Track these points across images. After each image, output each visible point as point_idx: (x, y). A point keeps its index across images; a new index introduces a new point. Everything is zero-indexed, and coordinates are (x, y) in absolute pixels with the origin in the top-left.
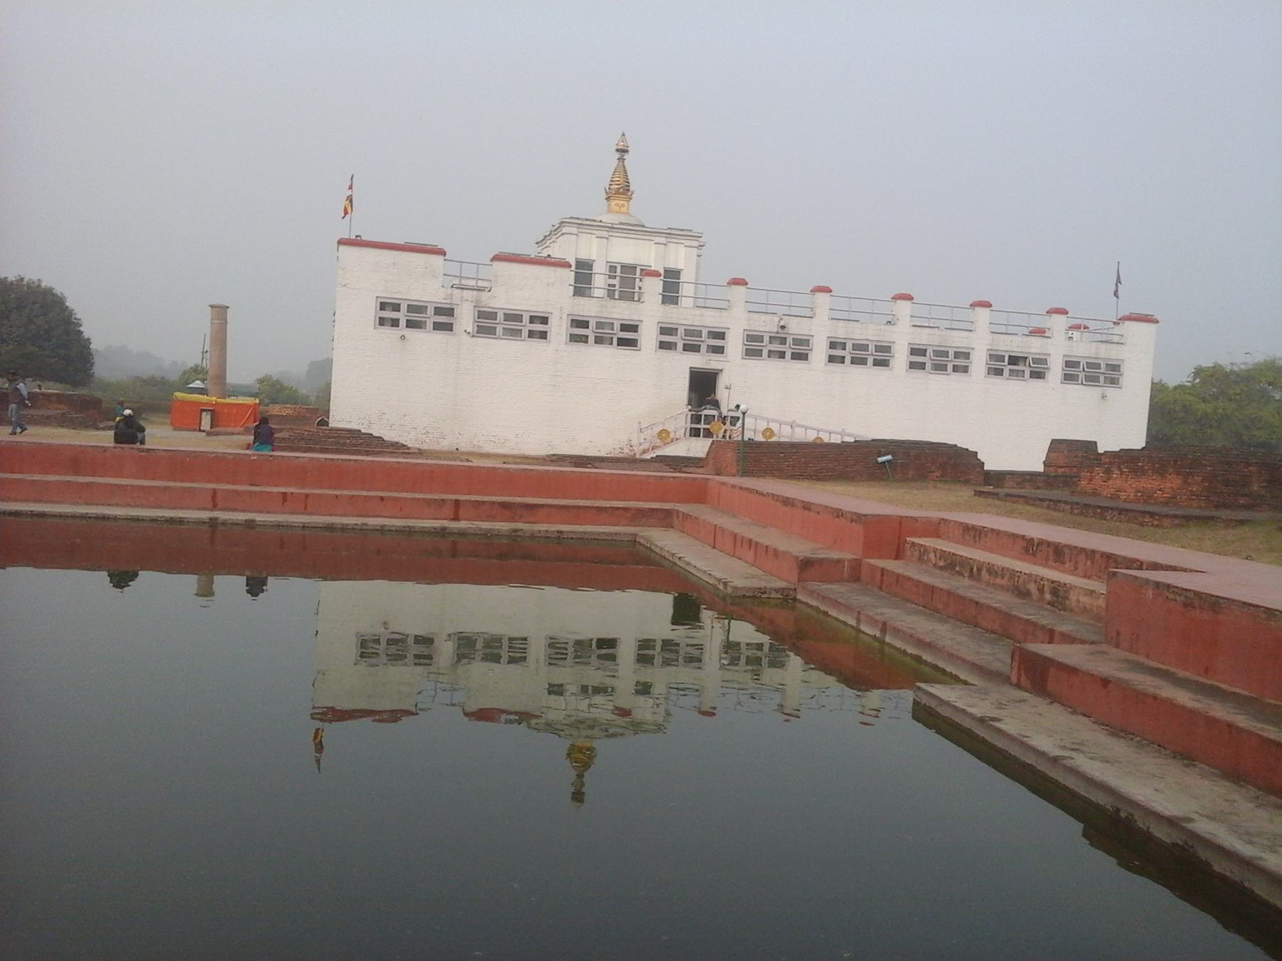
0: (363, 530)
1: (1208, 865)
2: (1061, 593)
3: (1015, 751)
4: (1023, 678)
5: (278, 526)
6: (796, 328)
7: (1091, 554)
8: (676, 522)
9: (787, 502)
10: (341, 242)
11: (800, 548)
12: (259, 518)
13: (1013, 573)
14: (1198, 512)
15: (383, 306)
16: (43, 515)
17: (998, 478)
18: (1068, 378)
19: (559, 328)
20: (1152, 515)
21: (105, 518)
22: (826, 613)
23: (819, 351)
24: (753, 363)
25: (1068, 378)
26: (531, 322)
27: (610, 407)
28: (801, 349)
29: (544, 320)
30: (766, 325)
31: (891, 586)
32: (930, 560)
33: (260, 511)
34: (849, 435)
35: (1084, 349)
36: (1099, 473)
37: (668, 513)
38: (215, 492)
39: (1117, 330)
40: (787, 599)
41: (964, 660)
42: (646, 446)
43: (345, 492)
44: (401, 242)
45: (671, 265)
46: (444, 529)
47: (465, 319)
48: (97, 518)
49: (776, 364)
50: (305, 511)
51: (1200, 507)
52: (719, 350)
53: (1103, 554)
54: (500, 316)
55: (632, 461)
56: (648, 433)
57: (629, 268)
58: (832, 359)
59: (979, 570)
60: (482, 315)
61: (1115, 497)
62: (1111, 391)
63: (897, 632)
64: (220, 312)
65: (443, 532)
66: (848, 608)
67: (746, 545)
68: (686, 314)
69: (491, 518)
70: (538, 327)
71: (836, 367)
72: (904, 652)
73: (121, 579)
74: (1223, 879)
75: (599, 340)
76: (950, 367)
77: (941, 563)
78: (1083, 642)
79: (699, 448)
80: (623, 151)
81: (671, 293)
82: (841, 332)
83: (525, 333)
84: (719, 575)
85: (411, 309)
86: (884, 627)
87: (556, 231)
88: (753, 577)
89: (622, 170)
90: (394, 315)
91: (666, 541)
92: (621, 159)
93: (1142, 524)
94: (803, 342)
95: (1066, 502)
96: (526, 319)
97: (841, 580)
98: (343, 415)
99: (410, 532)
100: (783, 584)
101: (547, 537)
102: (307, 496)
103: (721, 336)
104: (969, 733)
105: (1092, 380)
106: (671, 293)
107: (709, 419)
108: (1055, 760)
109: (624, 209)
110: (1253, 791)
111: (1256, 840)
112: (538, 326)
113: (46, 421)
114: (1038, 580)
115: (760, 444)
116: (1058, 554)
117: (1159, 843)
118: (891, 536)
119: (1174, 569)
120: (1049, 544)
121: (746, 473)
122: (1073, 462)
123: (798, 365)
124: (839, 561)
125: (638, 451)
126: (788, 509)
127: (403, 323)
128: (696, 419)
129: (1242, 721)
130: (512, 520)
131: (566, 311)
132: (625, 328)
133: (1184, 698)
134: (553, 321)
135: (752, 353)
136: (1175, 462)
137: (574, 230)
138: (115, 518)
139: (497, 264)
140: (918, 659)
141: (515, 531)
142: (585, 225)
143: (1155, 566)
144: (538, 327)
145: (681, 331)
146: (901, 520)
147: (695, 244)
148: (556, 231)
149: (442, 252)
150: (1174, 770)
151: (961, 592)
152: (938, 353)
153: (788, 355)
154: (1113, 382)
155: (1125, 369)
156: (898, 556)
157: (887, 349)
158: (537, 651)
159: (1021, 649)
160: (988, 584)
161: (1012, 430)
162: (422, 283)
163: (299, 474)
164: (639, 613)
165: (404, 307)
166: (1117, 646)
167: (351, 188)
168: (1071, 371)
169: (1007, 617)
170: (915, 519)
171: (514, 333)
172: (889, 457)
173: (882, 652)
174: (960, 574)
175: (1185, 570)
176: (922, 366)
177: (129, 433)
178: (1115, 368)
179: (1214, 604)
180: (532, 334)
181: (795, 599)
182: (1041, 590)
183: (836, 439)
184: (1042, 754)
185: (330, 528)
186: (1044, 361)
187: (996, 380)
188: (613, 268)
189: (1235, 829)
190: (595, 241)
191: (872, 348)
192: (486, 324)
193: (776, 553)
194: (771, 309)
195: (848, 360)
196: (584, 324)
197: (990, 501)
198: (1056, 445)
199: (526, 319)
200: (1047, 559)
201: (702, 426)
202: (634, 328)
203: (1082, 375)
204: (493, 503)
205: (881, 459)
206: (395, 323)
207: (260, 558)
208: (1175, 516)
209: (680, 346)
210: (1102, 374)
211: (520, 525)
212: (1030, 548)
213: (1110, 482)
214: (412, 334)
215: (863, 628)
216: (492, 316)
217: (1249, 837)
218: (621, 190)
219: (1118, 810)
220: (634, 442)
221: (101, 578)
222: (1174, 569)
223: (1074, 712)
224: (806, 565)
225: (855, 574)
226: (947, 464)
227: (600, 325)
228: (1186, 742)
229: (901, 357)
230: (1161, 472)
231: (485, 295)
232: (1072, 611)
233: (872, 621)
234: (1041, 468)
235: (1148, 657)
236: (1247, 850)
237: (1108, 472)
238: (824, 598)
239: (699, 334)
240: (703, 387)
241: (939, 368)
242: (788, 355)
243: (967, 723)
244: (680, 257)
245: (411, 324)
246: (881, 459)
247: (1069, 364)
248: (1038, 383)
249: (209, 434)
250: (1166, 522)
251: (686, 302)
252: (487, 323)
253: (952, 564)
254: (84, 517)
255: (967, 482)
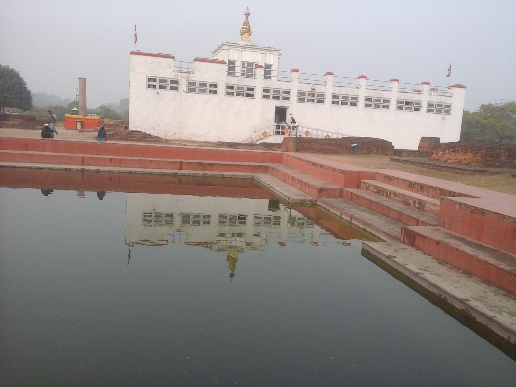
0: (143, 174)
1: (475, 318)
2: (422, 204)
3: (401, 270)
4: (406, 239)
5: (109, 172)
6: (319, 89)
7: (435, 189)
8: (269, 171)
9: (314, 164)
10: (132, 53)
11: (319, 183)
12: (102, 168)
13: (404, 196)
14: (479, 169)
15: (149, 80)
16: (14, 167)
17: (400, 153)
18: (429, 111)
19: (222, 89)
20: (461, 169)
21: (39, 168)
22: (328, 210)
23: (328, 99)
24: (301, 104)
25: (429, 111)
26: (210, 87)
27: (243, 122)
28: (321, 98)
29: (216, 86)
30: (307, 88)
31: (355, 199)
32: (371, 189)
33: (101, 166)
34: (340, 134)
35: (436, 99)
36: (440, 152)
37: (266, 167)
38: (83, 158)
39: (449, 91)
40: (314, 204)
41: (382, 231)
42: (257, 138)
43: (136, 158)
44: (156, 53)
45: (268, 63)
46: (176, 173)
47: (183, 85)
48: (36, 168)
49: (310, 104)
50: (120, 166)
51: (480, 166)
52: (287, 99)
53: (439, 189)
54: (198, 84)
55: (251, 145)
56: (258, 133)
57: (250, 64)
58: (333, 103)
59: (390, 194)
60: (190, 83)
61: (446, 162)
62: (446, 116)
63: (356, 219)
64: (83, 81)
65: (175, 175)
66: (337, 209)
67: (297, 181)
68: (273, 84)
69: (194, 169)
70: (213, 89)
71: (335, 106)
72: (359, 227)
73: (46, 192)
74: (480, 324)
75: (238, 94)
76: (381, 106)
77: (375, 191)
78: (430, 225)
79: (279, 139)
80: (247, 15)
81: (267, 75)
82: (337, 91)
83: (208, 91)
84: (286, 194)
85: (161, 81)
86: (352, 217)
87: (220, 48)
88: (300, 195)
89: (247, 23)
90: (154, 83)
91: (265, 179)
92: (247, 18)
93: (457, 173)
94: (322, 95)
95: (426, 164)
97: (335, 197)
98: (134, 125)
99: (162, 174)
100: (311, 198)
101: (217, 177)
102: (120, 160)
103: (288, 93)
104: (383, 262)
105: (439, 111)
106: (267, 75)
107: (283, 127)
108: (417, 274)
109: (248, 39)
110: (494, 288)
111: (493, 309)
112: (213, 89)
113: (14, 126)
114: (413, 199)
115: (304, 139)
116: (421, 188)
117: (456, 309)
118: (355, 179)
119: (468, 196)
120: (418, 184)
121: (297, 151)
122: (430, 145)
123: (320, 105)
124: (334, 189)
125: (254, 140)
126: (314, 167)
127: (158, 87)
128: (278, 127)
129: (491, 260)
130: (203, 170)
131: (224, 82)
132: (249, 89)
133: (469, 250)
134: (219, 86)
135: (301, 100)
136: (471, 147)
137: (228, 48)
138: (43, 168)
139: (196, 63)
140: (365, 230)
141: (205, 174)
142: (232, 46)
143: (460, 195)
144: (213, 89)
145: (272, 91)
146: (359, 173)
147: (278, 54)
148: (220, 48)
149: (173, 57)
150: (464, 279)
151: (383, 203)
152: (377, 100)
153: (316, 101)
154: (448, 112)
155: (452, 107)
156: (358, 187)
157: (356, 98)
158: (215, 220)
159: (405, 228)
160: (394, 199)
161: (405, 132)
162: (165, 70)
163: (117, 150)
164: (255, 207)
165: (158, 80)
166: (444, 227)
167: (135, 30)
168: (430, 108)
169: (401, 213)
170: (365, 172)
171: (204, 91)
172: (356, 144)
173: (350, 226)
174: (383, 195)
175: (472, 197)
176: (370, 106)
177: (48, 133)
178: (448, 106)
179: (482, 212)
180: (210, 92)
181: (316, 204)
182: (414, 203)
183: (334, 136)
184: (412, 272)
185: (130, 173)
186: (420, 104)
187: (400, 111)
188: (243, 64)
189: (486, 304)
190: (236, 52)
191: (350, 98)
192: (192, 87)
193: (309, 186)
194: (309, 82)
195: (340, 103)
196: (232, 88)
197: (396, 163)
198: (423, 139)
199: (208, 85)
200: (417, 190)
201: (280, 130)
202: (252, 89)
203: (435, 110)
204: (196, 163)
205: (352, 145)
206: (154, 87)
207: (102, 184)
208: (470, 170)
209: (271, 97)
210: (443, 109)
211: (207, 172)
212: (411, 185)
213: (445, 155)
214: (161, 91)
215: (343, 217)
216: (194, 84)
217: (491, 308)
218: (247, 31)
219: (441, 295)
220: (253, 137)
221: (38, 192)
222: (468, 196)
223: (425, 254)
224: (321, 190)
225: (341, 194)
226: (378, 147)
227: (238, 88)
228: (469, 268)
229: (361, 102)
230: (465, 152)
231: (191, 76)
232: (426, 211)
233: (347, 214)
234: (417, 149)
235: (456, 232)
236: (490, 313)
237: (444, 151)
238: (328, 204)
239: (279, 92)
240: (281, 113)
241: (377, 106)
242: (316, 101)
243: (383, 258)
244: (271, 59)
245: (161, 87)
246: (352, 145)
247: (430, 105)
248: (417, 113)
249: (80, 131)
250: (466, 172)
251: (274, 79)
252: (192, 87)
253: (379, 191)
254: (31, 168)
255: (387, 155)
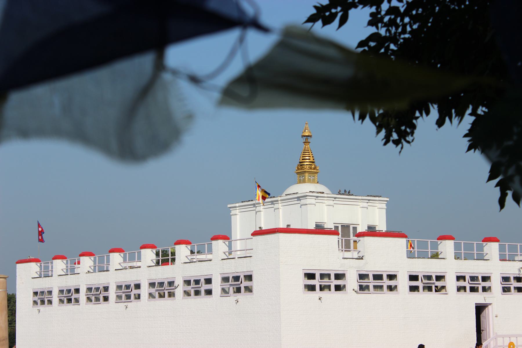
29: (391, 277)
47: (351, 282)
85: (322, 276)
90: (311, 282)
96: (385, 277)
127: (318, 288)
135: (506, 290)
165: (318, 276)
206: (312, 288)
245: (322, 289)
